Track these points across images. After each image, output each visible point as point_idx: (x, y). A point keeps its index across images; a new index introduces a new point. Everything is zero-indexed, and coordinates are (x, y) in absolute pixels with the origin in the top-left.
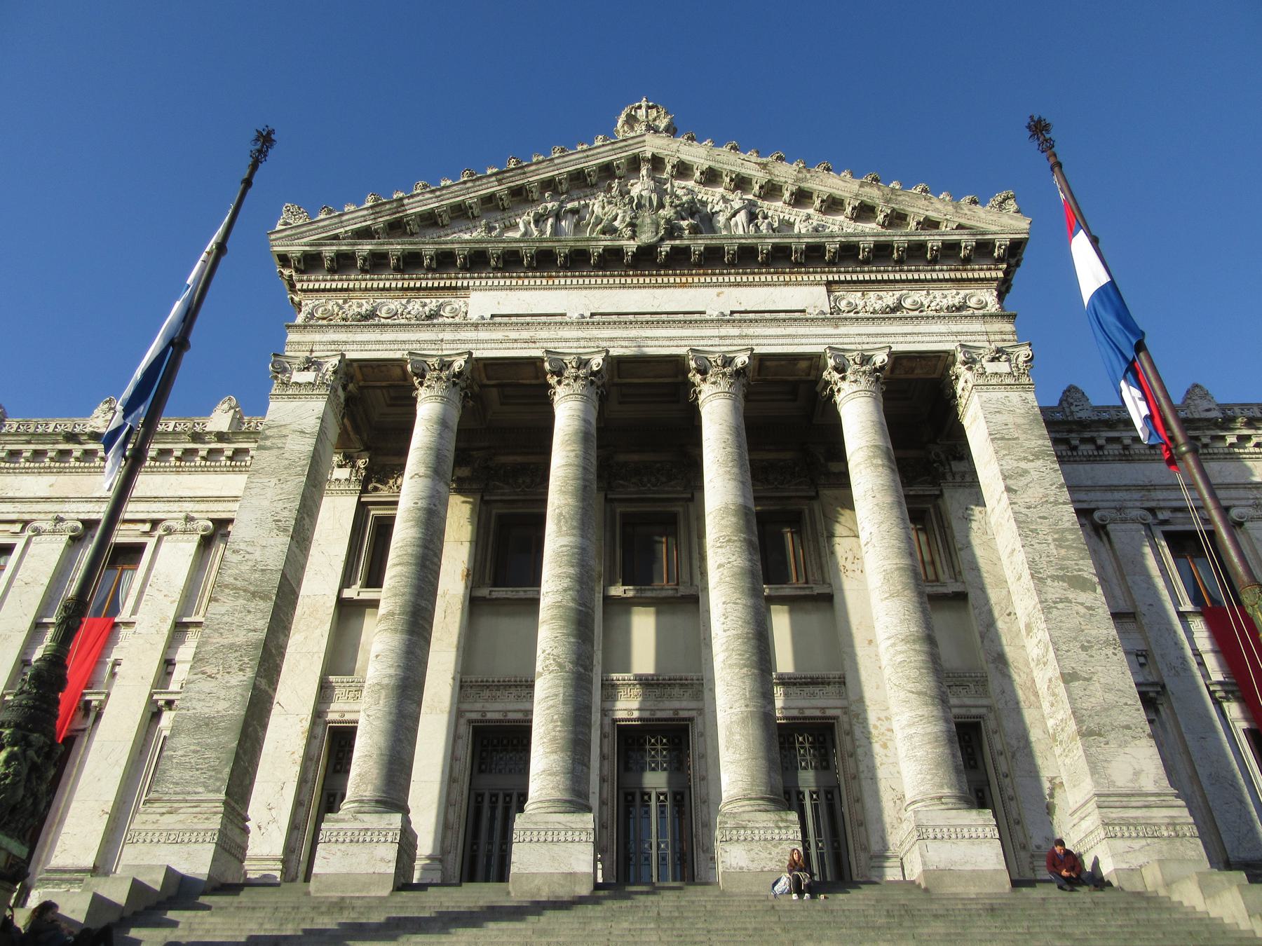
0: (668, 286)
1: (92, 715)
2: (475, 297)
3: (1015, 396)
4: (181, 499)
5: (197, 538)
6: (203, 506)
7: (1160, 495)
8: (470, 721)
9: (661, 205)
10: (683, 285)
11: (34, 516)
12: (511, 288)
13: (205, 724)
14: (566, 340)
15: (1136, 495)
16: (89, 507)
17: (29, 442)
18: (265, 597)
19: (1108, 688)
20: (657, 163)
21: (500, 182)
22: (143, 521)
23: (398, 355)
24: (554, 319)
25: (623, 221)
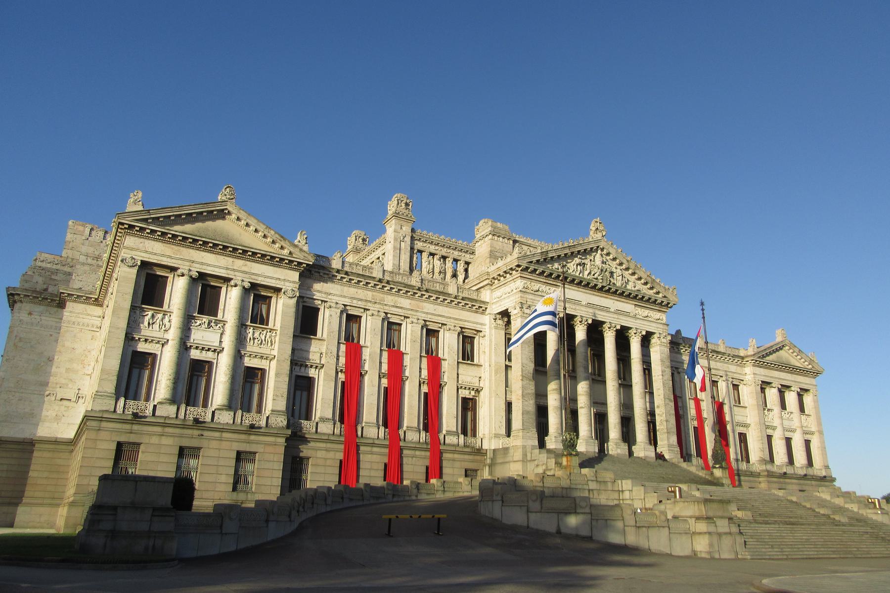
16: (424, 315)
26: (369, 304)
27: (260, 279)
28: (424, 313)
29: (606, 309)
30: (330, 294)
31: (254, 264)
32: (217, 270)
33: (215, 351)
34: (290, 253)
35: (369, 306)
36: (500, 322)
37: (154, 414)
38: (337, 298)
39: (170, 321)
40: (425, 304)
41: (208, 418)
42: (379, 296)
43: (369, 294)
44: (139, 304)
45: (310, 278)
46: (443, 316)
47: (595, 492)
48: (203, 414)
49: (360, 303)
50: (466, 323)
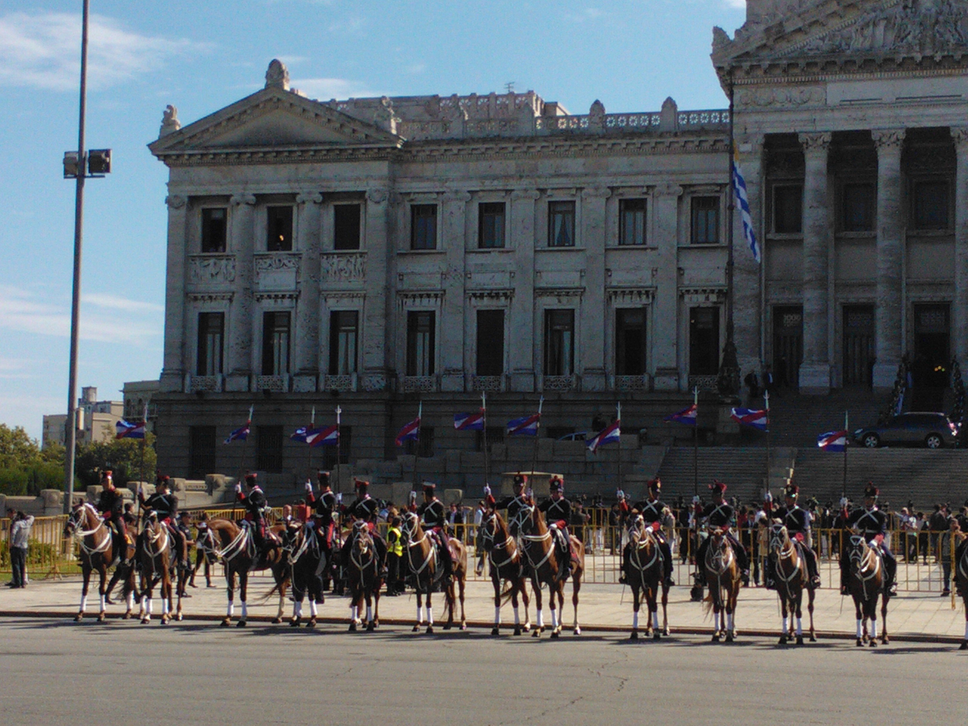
1: (650, 296)
2: (830, 86)
4: (660, 173)
5: (676, 198)
6: (674, 177)
8: (841, 304)
9: (937, 22)
10: (950, 75)
11: (583, 186)
12: (849, 81)
14: (881, 117)
16: (610, 179)
17: (566, 140)
18: (755, 273)
22: (642, 187)
23: (792, 131)
25: (914, 37)
26: (512, 182)
31: (323, 165)
33: (291, 297)
34: (367, 136)
35: (513, 184)
37: (224, 391)
39: (234, 267)
40: (611, 159)
41: (286, 388)
43: (511, 166)
44: (197, 250)
45: (414, 162)
46: (646, 173)
48: (279, 383)
49: (496, 182)
50: (695, 176)
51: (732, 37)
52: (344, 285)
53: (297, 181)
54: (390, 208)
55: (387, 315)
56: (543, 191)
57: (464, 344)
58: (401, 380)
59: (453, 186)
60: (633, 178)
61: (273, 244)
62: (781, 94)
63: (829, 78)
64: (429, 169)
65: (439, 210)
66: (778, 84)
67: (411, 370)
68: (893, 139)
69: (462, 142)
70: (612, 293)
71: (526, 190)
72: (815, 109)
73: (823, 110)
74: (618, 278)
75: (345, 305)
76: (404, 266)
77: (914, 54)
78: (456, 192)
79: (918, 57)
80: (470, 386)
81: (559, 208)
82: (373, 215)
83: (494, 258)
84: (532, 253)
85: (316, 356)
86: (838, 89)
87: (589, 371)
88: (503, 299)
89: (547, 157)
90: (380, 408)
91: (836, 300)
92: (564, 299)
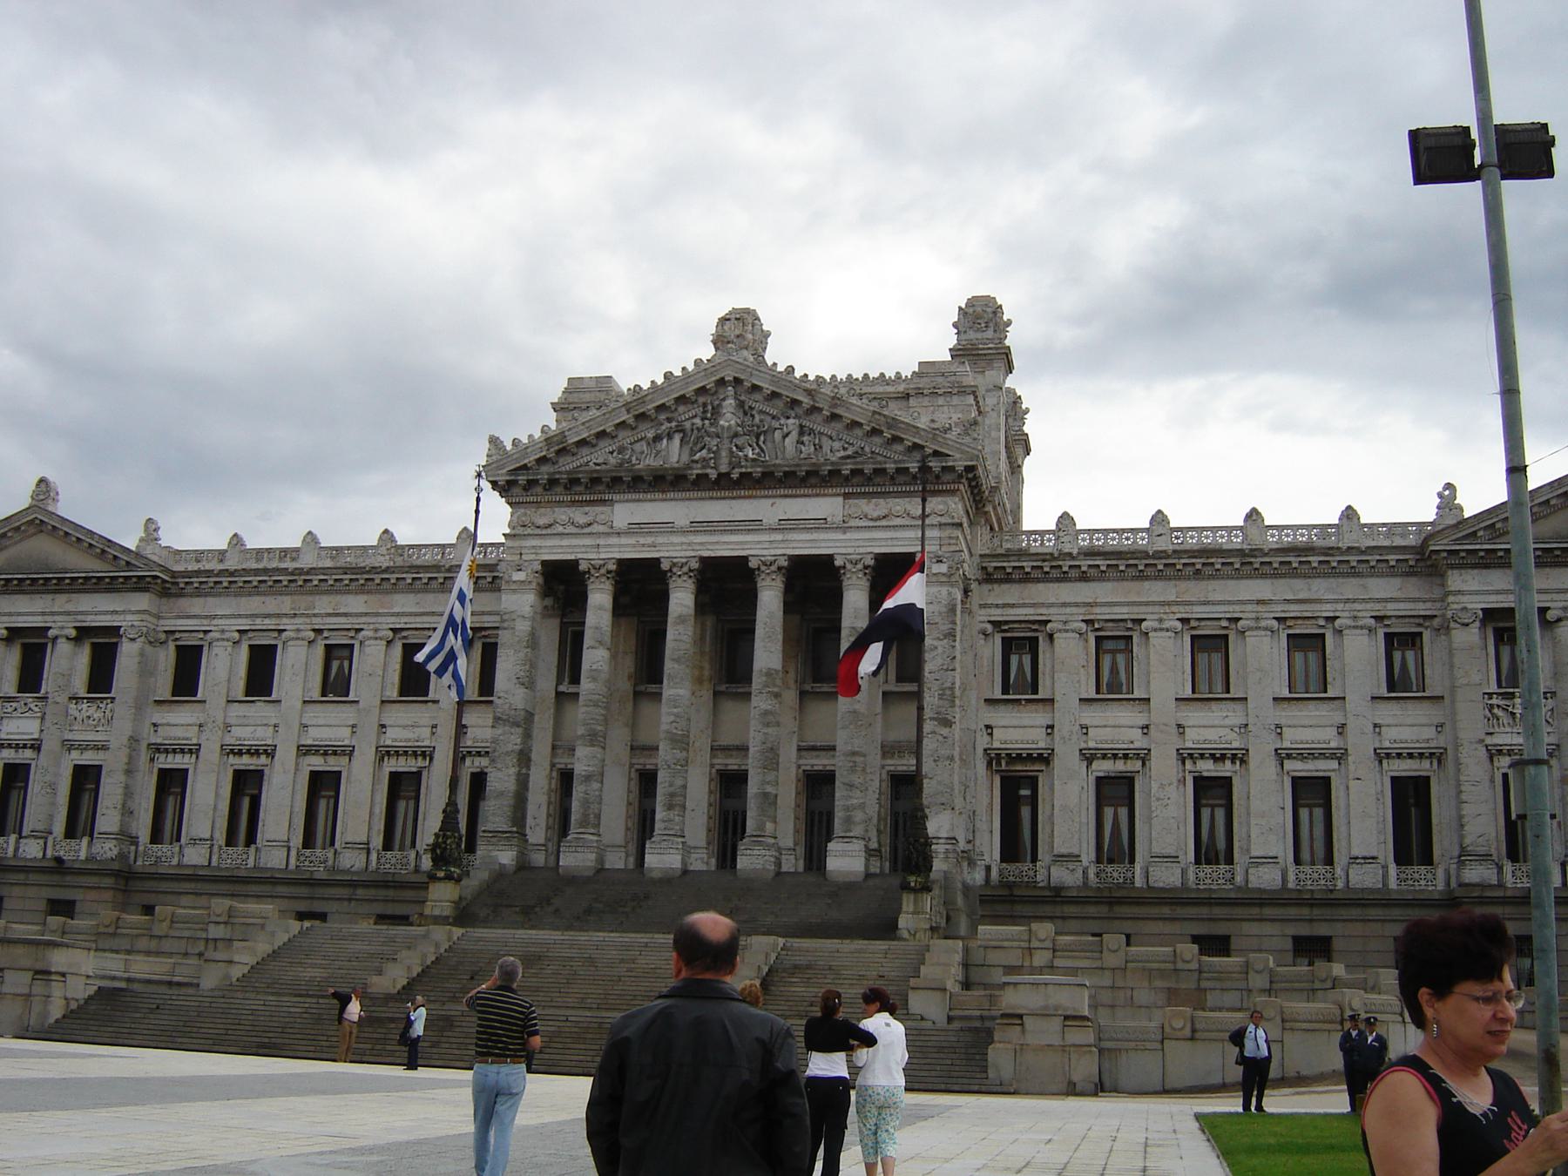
0: (740, 497)
2: (617, 507)
3: (944, 590)
7: (1097, 610)
9: (736, 435)
10: (750, 497)
13: (501, 794)
14: (672, 544)
15: (1082, 610)
16: (393, 619)
19: (939, 783)
20: (737, 381)
21: (628, 411)
24: (668, 528)
25: (709, 450)
26: (285, 620)
27: (89, 618)
28: (393, 615)
29: (754, 526)
30: (215, 617)
32: (30, 618)
33: (32, 747)
35: (285, 623)
36: (549, 601)
38: (228, 622)
40: (397, 597)
42: (303, 602)
43: (285, 604)
45: (181, 595)
47: (220, 944)
49: (267, 621)
50: (486, 618)
51: (509, 447)
52: (90, 736)
53: (53, 614)
54: (149, 648)
55: (129, 772)
56: (318, 631)
57: (215, 808)
58: (141, 848)
59: (222, 623)
60: (418, 619)
61: (22, 688)
62: (562, 514)
63: (616, 497)
64: (197, 605)
65: (205, 649)
66: (560, 503)
67: (156, 837)
68: (685, 569)
69: (232, 574)
70: (384, 753)
71: (298, 630)
72: (599, 534)
73: (608, 534)
74: (393, 737)
75: (89, 758)
76: (160, 716)
77: (709, 471)
78: (223, 631)
79: (713, 475)
80: (214, 863)
81: (337, 653)
82: (128, 656)
83: (259, 710)
84: (299, 704)
85: (51, 817)
86: (625, 512)
87: (349, 845)
88: (263, 757)
89: (328, 592)
90: (108, 881)
91: (632, 765)
92: (332, 760)
